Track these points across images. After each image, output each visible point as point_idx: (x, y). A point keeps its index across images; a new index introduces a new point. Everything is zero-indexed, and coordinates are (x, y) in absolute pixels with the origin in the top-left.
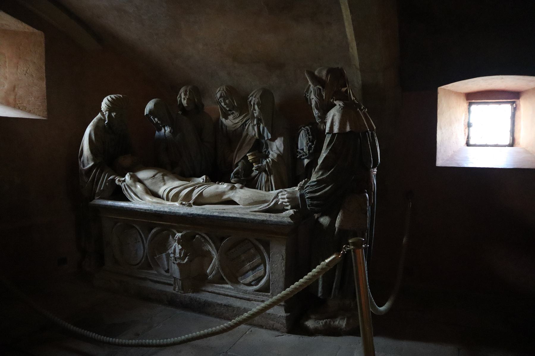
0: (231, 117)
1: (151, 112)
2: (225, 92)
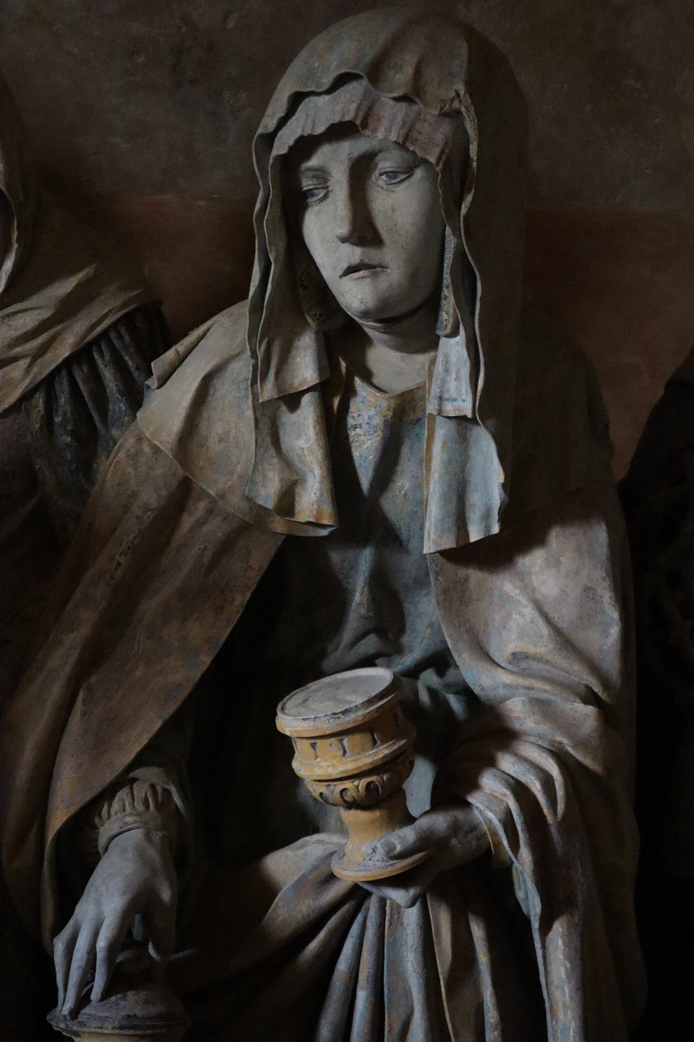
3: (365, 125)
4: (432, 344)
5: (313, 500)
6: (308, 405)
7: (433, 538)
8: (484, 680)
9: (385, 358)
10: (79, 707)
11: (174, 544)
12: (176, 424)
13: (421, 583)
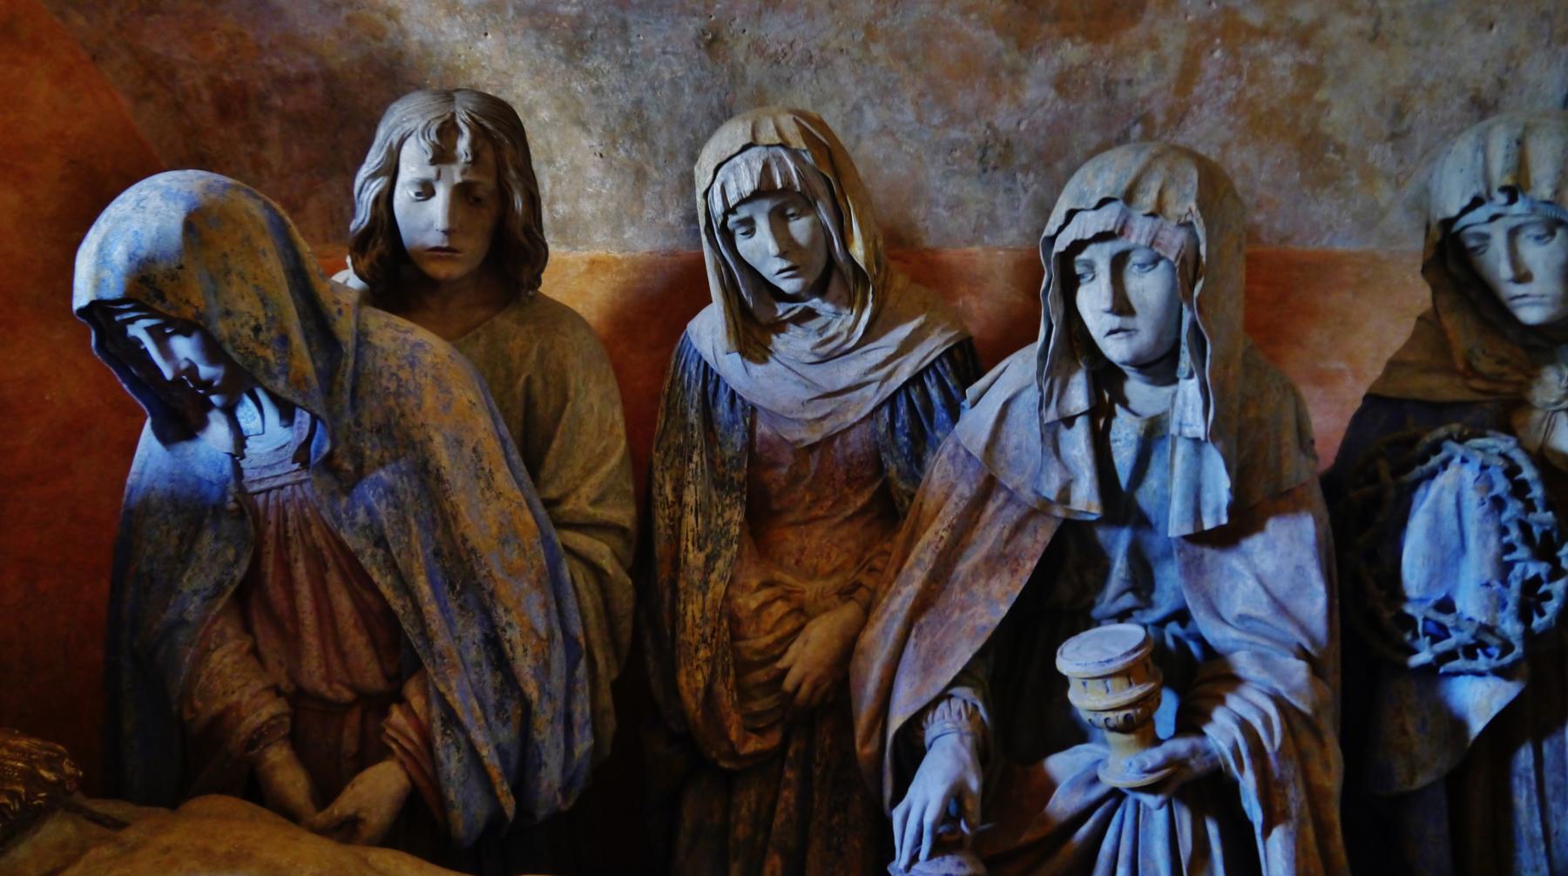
0: (794, 344)
1: (149, 285)
2: (795, 155)
3: (1122, 233)
4: (1175, 381)
5: (1085, 497)
6: (1081, 430)
7: (1177, 525)
8: (1216, 634)
9: (1136, 388)
10: (912, 640)
11: (982, 523)
12: (984, 437)
13: (1167, 555)
